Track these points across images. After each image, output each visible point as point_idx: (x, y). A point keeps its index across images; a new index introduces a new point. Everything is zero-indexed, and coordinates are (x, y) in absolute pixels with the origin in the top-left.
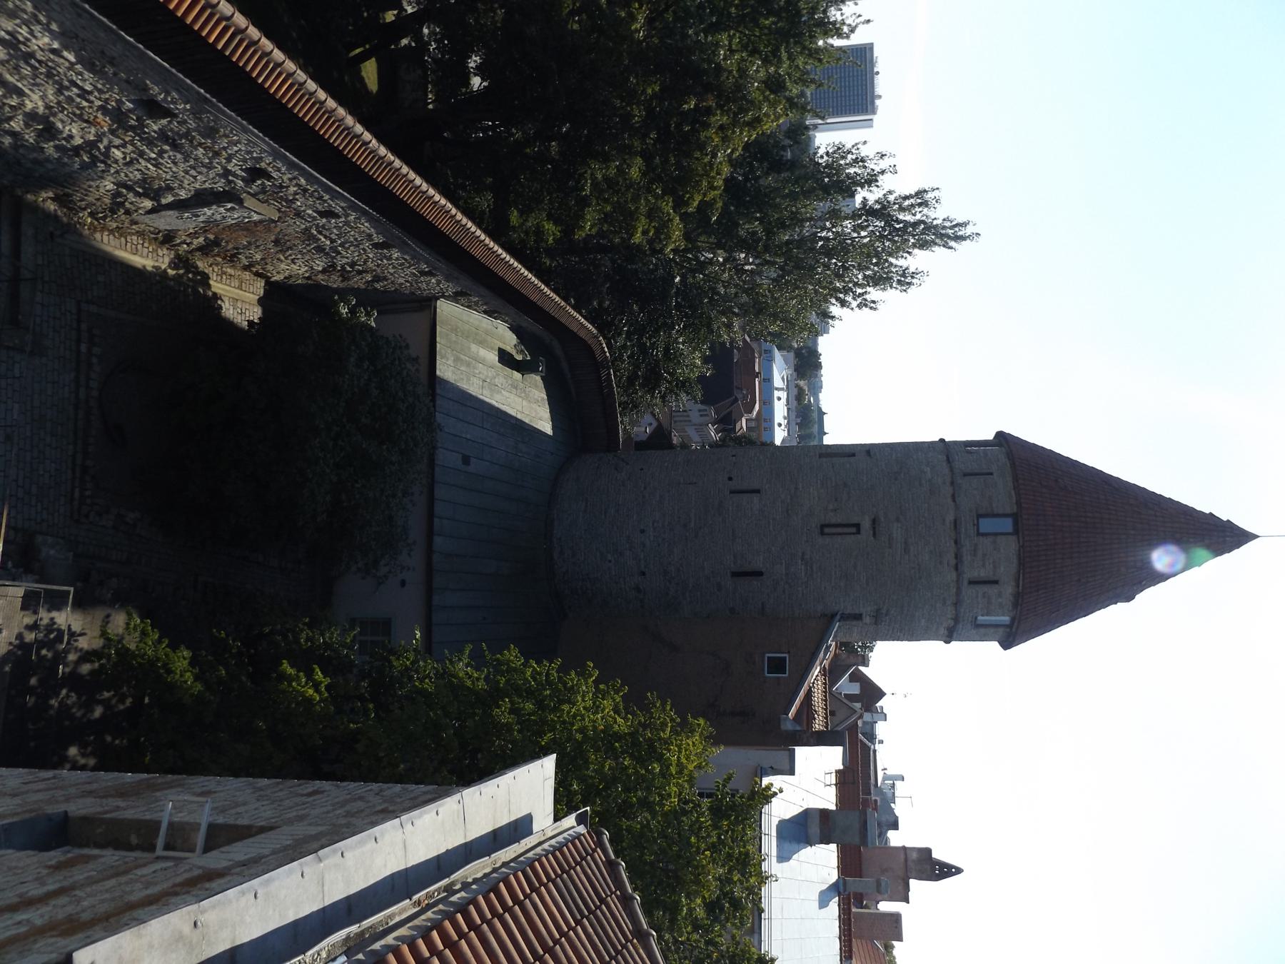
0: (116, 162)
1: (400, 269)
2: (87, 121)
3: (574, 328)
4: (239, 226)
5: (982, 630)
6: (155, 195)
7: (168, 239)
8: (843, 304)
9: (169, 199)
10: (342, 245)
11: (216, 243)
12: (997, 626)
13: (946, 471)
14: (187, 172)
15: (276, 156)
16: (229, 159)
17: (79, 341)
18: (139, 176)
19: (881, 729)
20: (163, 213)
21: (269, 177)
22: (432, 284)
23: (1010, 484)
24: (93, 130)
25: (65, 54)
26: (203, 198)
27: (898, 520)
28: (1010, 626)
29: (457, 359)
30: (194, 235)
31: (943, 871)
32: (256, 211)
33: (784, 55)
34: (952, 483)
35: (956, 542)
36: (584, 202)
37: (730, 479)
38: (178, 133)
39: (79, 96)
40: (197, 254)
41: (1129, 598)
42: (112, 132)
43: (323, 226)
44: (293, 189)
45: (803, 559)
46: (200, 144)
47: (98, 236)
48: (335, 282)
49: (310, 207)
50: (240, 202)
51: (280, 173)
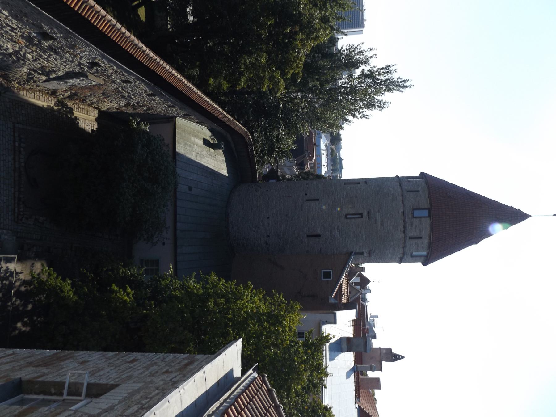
0: (29, 60)
1: (160, 105)
2: (15, 42)
3: (237, 129)
4: (86, 87)
5: (415, 258)
6: (47, 74)
7: (53, 93)
8: (354, 116)
9: (54, 76)
10: (133, 95)
11: (76, 94)
12: (421, 256)
13: (400, 190)
14: (62, 64)
15: (103, 57)
16: (81, 58)
17: (14, 141)
18: (39, 66)
19: (369, 296)
20: (51, 82)
21: (100, 66)
22: (173, 111)
23: (427, 196)
24: (17, 46)
25: (3, 12)
26: (69, 75)
27: (379, 211)
28: (427, 256)
29: (185, 144)
30: (66, 91)
31: (397, 358)
32: (94, 80)
33: (329, 7)
34: (402, 195)
35: (404, 221)
36: (241, 74)
37: (306, 194)
38: (57, 47)
39: (10, 30)
40: (67, 99)
41: (477, 243)
42: (27, 46)
43: (124, 87)
44: (110, 71)
45: (338, 229)
46: (68, 52)
47: (21, 92)
48: (130, 110)
49: (119, 79)
50: (87, 77)
51: (105, 64)
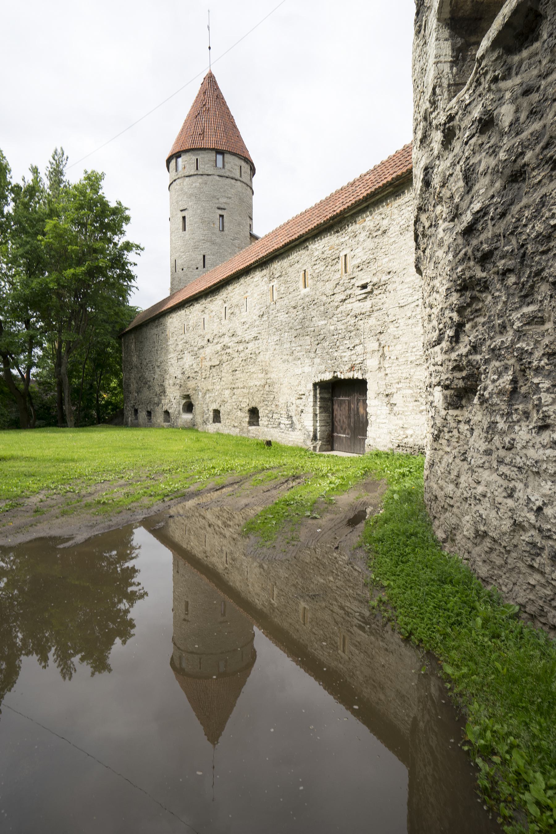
13: (195, 177)
27: (218, 199)
34: (202, 175)
37: (197, 268)
